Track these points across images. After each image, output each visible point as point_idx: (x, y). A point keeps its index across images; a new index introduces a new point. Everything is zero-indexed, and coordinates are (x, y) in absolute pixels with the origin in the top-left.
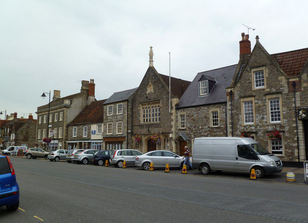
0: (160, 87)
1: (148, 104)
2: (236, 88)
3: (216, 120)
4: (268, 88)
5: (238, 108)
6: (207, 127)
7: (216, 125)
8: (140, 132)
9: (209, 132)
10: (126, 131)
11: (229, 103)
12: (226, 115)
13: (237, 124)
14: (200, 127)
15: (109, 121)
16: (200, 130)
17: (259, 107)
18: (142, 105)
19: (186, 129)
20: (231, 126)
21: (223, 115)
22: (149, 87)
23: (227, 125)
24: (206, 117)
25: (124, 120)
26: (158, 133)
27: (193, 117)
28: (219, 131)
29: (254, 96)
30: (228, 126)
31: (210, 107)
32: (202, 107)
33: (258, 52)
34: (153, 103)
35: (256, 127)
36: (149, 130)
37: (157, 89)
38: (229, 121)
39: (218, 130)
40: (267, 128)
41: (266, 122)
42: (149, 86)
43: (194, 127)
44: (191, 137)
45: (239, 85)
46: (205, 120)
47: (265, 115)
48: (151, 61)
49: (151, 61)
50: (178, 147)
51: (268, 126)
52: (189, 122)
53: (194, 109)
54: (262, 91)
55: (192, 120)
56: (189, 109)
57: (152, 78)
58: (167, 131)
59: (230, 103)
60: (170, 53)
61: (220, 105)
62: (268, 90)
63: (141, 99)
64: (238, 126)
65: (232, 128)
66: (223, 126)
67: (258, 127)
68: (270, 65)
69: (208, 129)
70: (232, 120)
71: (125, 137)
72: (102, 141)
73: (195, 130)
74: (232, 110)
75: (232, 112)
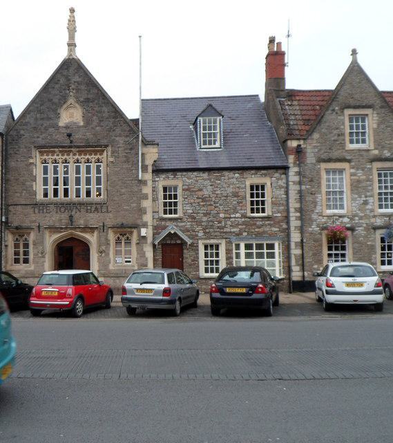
0: (106, 115)
1: (60, 152)
2: (309, 141)
4: (376, 149)
5: (315, 181)
6: (238, 215)
8: (35, 221)
9: (244, 227)
11: (293, 170)
12: (287, 193)
13: (313, 211)
14: (222, 215)
16: (220, 222)
17: (359, 181)
18: (42, 153)
19: (181, 219)
20: (298, 214)
21: (278, 192)
22: (68, 107)
23: (288, 211)
24: (236, 195)
26: (102, 224)
27: (200, 193)
28: (269, 224)
29: (349, 161)
30: (291, 214)
31: (247, 174)
32: (226, 173)
33: (358, 81)
34: (80, 153)
35: (352, 219)
36: (71, 217)
37: (95, 117)
38: (294, 204)
39: (267, 223)
40: (373, 220)
41: (372, 211)
42: (65, 106)
43: (205, 215)
44: (197, 236)
45: (316, 136)
46: (234, 201)
47: (370, 196)
48: (72, 45)
49: (72, 45)
50: (159, 257)
51: (374, 216)
52: (191, 204)
53: (205, 175)
54: (363, 153)
55: (200, 198)
56: (190, 173)
57: (78, 90)
58: (129, 220)
59: (296, 169)
60: (140, 37)
61: (270, 171)
62: (376, 152)
63: (38, 137)
64: (314, 216)
65: (301, 218)
66: (279, 215)
67: (357, 218)
68: (382, 107)
69: (243, 220)
70: (301, 203)
73: (208, 221)
74: (300, 183)
75: (301, 187)
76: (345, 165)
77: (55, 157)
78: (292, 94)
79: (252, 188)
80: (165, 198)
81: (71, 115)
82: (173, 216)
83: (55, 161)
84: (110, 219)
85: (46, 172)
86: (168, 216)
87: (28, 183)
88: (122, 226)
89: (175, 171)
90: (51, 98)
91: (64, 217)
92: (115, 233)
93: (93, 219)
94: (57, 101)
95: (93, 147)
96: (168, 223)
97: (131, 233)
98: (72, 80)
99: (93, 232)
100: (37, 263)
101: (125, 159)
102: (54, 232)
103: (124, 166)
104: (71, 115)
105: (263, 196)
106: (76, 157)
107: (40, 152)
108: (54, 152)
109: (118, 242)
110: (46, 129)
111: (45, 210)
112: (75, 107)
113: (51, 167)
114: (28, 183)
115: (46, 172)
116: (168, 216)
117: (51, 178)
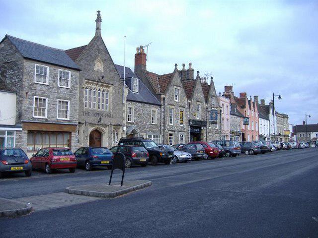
11: (163, 107)
12: (161, 115)
15: (38, 92)
25: (73, 99)
27: (139, 112)
34: (101, 85)
45: (167, 94)
63: (86, 74)
72: (21, 129)
76: (173, 107)
78: (148, 73)
97: (119, 128)
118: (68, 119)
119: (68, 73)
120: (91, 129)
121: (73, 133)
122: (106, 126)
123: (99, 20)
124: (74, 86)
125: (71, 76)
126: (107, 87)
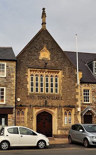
0: (60, 56)
3: (86, 97)
7: (86, 101)
8: (28, 103)
10: (14, 101)
25: (9, 86)
34: (48, 72)
36: (46, 101)
37: (55, 57)
42: (42, 51)
48: (44, 23)
49: (44, 23)
50: (83, 121)
63: (30, 63)
71: (13, 108)
77: (37, 73)
79: (84, 90)
80: (88, 97)
81: (45, 55)
82: (87, 103)
83: (37, 75)
84: (62, 103)
85: (32, 80)
86: (85, 103)
87: (25, 85)
88: (69, 106)
89: (88, 83)
90: (36, 46)
91: (42, 102)
92: (65, 109)
93: (55, 103)
94: (38, 47)
95: (54, 69)
96: (86, 106)
97: (71, 110)
98: (43, 38)
99: (55, 109)
100: (29, 123)
101: (69, 76)
102: (37, 108)
103: (68, 80)
104: (45, 55)
105: (88, 95)
106: (47, 74)
107: (30, 70)
108: (37, 71)
109: (66, 114)
110: (33, 60)
111: (33, 98)
112: (46, 51)
113: (34, 78)
114: (25, 85)
115: (32, 80)
116: (85, 103)
117: (54, 84)
118: (4, 103)
119: (4, 65)
120: (36, 111)
121: (9, 115)
122: (52, 107)
123: (44, 15)
124: (10, 75)
125: (7, 66)
126: (55, 72)
